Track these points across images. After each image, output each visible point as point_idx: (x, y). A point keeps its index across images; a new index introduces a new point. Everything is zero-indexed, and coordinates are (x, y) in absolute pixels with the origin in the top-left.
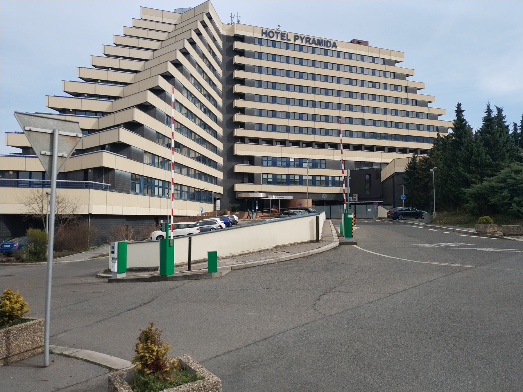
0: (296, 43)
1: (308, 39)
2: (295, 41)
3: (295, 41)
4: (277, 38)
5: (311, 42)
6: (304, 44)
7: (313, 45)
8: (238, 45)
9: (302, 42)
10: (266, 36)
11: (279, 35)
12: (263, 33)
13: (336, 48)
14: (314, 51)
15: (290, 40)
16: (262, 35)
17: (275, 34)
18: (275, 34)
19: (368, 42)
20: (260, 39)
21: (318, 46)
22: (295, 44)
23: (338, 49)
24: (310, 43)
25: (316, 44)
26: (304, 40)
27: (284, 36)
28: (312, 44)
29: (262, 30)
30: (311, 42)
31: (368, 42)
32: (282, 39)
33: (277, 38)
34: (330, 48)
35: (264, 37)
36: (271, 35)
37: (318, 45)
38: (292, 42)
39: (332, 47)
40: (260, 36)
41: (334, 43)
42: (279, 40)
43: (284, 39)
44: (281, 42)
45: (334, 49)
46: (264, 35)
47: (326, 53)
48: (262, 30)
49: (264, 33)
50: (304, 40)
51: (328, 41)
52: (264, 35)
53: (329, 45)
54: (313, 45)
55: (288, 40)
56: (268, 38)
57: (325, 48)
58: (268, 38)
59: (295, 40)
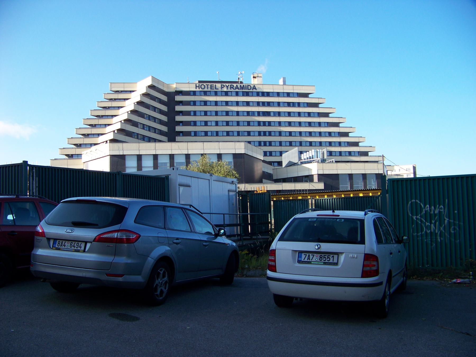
0: (222, 90)
1: (232, 86)
2: (222, 89)
3: (222, 89)
4: (208, 89)
5: (234, 88)
6: (229, 90)
7: (237, 90)
8: (178, 98)
9: (227, 89)
10: (199, 89)
12: (196, 87)
13: (256, 89)
14: (237, 94)
15: (218, 89)
16: (196, 88)
19: (285, 77)
21: (241, 90)
22: (221, 91)
24: (233, 89)
25: (239, 89)
27: (213, 87)
28: (235, 89)
29: (196, 85)
30: (234, 88)
31: (285, 77)
32: (211, 89)
33: (208, 89)
34: (251, 91)
35: (198, 89)
36: (203, 87)
37: (240, 89)
38: (220, 90)
39: (253, 90)
40: (194, 90)
41: (254, 86)
42: (209, 90)
43: (214, 89)
44: (210, 91)
45: (254, 90)
46: (198, 88)
48: (196, 85)
49: (198, 87)
51: (248, 86)
52: (198, 88)
53: (249, 87)
55: (216, 89)
56: (201, 90)
57: (247, 91)
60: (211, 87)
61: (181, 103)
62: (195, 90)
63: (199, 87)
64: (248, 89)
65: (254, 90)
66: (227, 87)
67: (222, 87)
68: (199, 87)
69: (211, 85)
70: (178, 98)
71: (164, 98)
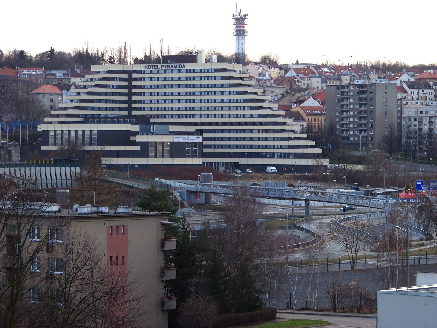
5: (170, 67)
6: (167, 69)
7: (172, 69)
8: (134, 76)
17: (152, 66)
18: (152, 66)
20: (144, 71)
21: (175, 69)
23: (186, 68)
26: (167, 67)
30: (170, 67)
32: (155, 68)
34: (182, 68)
45: (184, 68)
46: (146, 68)
47: (179, 71)
50: (167, 67)
52: (146, 68)
53: (180, 66)
54: (172, 69)
55: (158, 68)
56: (148, 69)
58: (148, 69)
60: (155, 67)
61: (136, 79)
62: (144, 69)
63: (147, 67)
64: (180, 68)
66: (166, 67)
67: (162, 67)
68: (147, 67)
69: (155, 65)
70: (134, 76)
71: (126, 76)
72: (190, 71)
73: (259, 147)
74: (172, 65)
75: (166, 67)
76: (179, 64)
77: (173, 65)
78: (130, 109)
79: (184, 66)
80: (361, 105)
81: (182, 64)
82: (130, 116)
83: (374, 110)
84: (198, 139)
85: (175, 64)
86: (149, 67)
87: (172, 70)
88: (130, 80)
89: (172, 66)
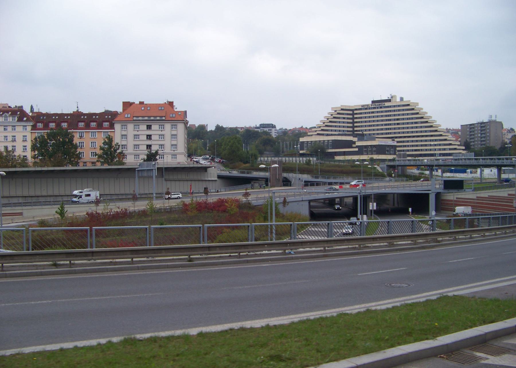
6: (374, 107)
7: (377, 106)
8: (355, 112)
11: (367, 106)
12: (362, 106)
23: (386, 105)
35: (362, 107)
38: (371, 107)
40: (361, 108)
42: (367, 107)
59: (371, 106)
61: (356, 114)
65: (384, 106)
66: (374, 105)
70: (355, 112)
71: (351, 112)
72: (388, 107)
73: (431, 150)
74: (377, 104)
75: (374, 105)
76: (381, 103)
77: (378, 104)
78: (353, 127)
79: (384, 104)
80: (481, 134)
81: (383, 103)
82: (353, 131)
83: (489, 136)
84: (395, 144)
85: (379, 104)
86: (364, 106)
87: (378, 107)
88: (353, 114)
89: (377, 105)
